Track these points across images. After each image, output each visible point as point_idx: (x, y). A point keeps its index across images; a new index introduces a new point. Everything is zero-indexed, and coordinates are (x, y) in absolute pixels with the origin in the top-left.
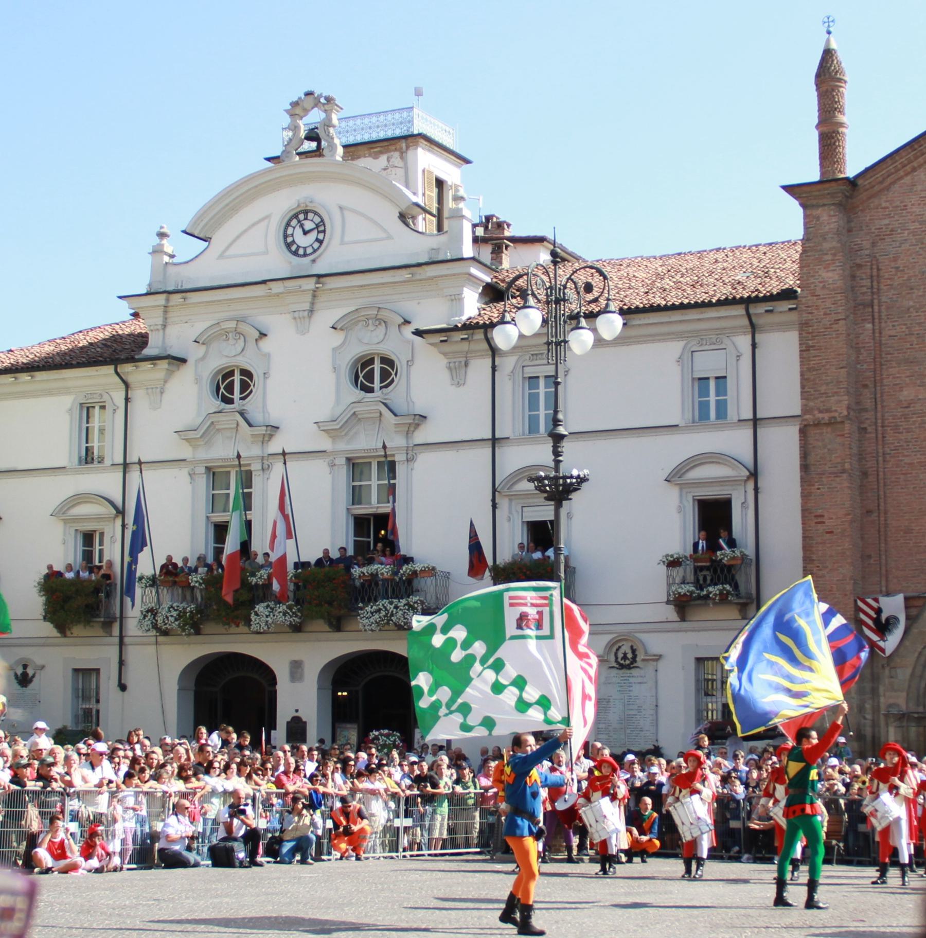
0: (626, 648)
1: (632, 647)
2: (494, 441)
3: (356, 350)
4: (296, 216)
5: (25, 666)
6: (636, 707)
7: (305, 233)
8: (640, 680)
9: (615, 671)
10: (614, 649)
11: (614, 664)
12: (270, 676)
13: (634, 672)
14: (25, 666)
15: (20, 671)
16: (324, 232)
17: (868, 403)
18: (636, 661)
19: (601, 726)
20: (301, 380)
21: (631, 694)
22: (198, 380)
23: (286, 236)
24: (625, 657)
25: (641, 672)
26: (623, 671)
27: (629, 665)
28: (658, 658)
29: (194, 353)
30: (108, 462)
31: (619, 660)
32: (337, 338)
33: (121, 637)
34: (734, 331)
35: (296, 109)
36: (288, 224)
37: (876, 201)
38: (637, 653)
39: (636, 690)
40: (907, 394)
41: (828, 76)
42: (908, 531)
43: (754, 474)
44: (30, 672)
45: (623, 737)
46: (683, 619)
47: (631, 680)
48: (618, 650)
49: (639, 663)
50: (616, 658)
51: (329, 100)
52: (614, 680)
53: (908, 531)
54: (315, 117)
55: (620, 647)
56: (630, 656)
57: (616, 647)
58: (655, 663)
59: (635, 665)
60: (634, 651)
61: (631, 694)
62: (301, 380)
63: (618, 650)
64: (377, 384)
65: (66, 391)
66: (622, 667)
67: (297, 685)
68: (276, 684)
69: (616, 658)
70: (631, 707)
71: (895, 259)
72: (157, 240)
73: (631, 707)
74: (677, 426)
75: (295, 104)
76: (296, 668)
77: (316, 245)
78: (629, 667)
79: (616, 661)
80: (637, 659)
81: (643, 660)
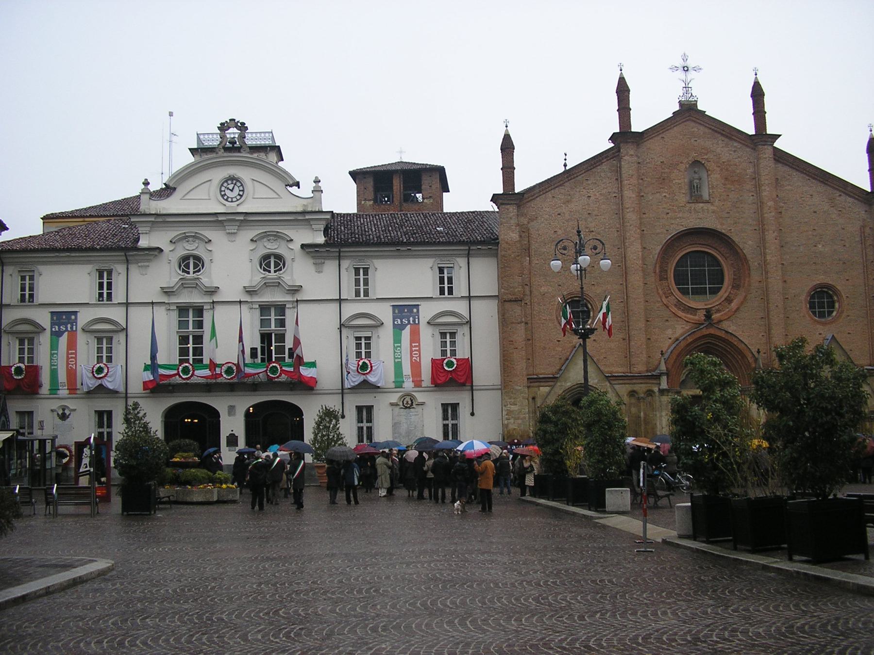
0: (408, 399)
2: (340, 301)
3: (263, 251)
4: (226, 181)
5: (64, 410)
7: (232, 191)
12: (216, 414)
14: (64, 410)
15: (60, 412)
16: (243, 191)
17: (528, 293)
20: (231, 266)
22: (170, 262)
23: (221, 191)
24: (407, 403)
28: (422, 404)
29: (166, 247)
30: (115, 301)
32: (253, 246)
33: (126, 393)
34: (459, 256)
35: (223, 127)
36: (222, 185)
37: (529, 204)
40: (543, 289)
41: (507, 147)
42: (545, 348)
43: (469, 322)
44: (67, 412)
49: (414, 406)
51: (243, 124)
53: (545, 348)
54: (233, 133)
62: (231, 266)
64: (272, 269)
65: (89, 262)
66: (406, 408)
67: (231, 418)
68: (219, 416)
71: (538, 230)
72: (143, 187)
75: (222, 124)
76: (232, 410)
77: (238, 197)
78: (409, 408)
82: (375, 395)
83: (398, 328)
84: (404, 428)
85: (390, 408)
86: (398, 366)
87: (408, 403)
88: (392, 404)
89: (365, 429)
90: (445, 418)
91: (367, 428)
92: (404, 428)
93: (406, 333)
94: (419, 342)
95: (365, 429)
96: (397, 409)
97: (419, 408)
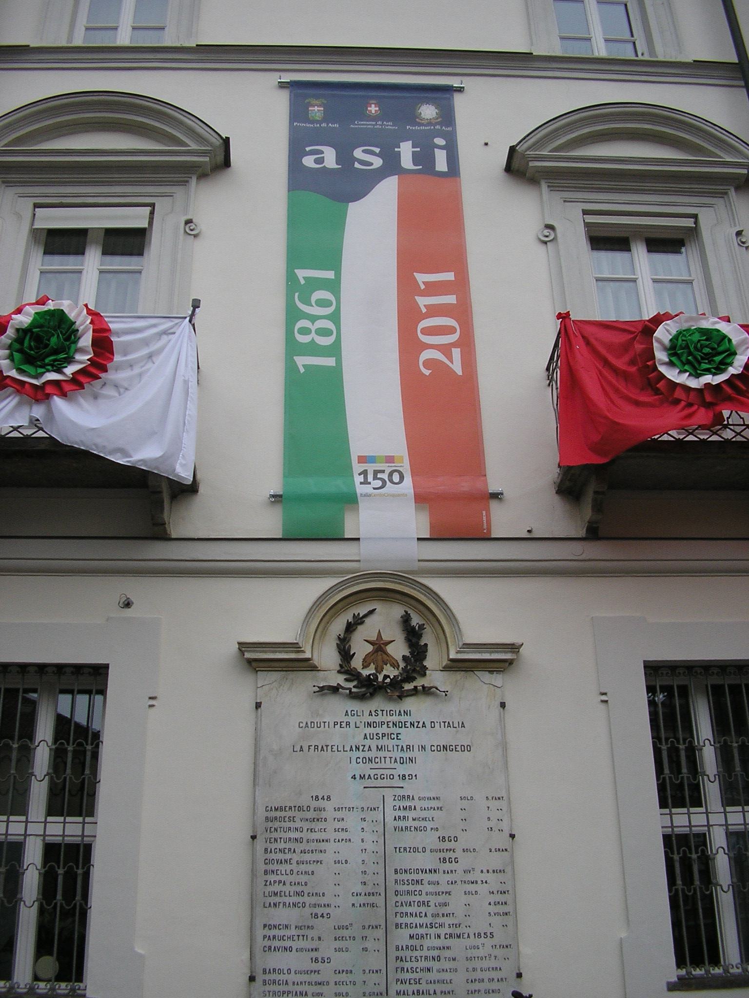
1: (406, 620)
8: (444, 736)
10: (338, 626)
11: (339, 679)
19: (281, 915)
25: (450, 710)
26: (377, 703)
31: (357, 663)
38: (428, 638)
39: (429, 775)
45: (376, 961)
46: (593, 534)
47: (408, 736)
48: (350, 628)
49: (435, 678)
50: (346, 655)
55: (359, 621)
56: (399, 650)
57: (347, 617)
58: (497, 679)
59: (419, 682)
60: (413, 635)
61: (409, 789)
63: (350, 628)
66: (368, 688)
69: (346, 655)
70: (409, 839)
73: (409, 839)
74: (526, 57)
78: (395, 689)
79: (346, 669)
80: (432, 661)
81: (456, 666)
82: (131, 587)
83: (321, 193)
84: (345, 860)
85: (243, 690)
86: (313, 400)
87: (388, 655)
89: (33, 855)
90: (677, 786)
91: (51, 851)
92: (345, 860)
93: (373, 223)
94: (456, 260)
95: (33, 855)
96: (292, 700)
97: (474, 697)
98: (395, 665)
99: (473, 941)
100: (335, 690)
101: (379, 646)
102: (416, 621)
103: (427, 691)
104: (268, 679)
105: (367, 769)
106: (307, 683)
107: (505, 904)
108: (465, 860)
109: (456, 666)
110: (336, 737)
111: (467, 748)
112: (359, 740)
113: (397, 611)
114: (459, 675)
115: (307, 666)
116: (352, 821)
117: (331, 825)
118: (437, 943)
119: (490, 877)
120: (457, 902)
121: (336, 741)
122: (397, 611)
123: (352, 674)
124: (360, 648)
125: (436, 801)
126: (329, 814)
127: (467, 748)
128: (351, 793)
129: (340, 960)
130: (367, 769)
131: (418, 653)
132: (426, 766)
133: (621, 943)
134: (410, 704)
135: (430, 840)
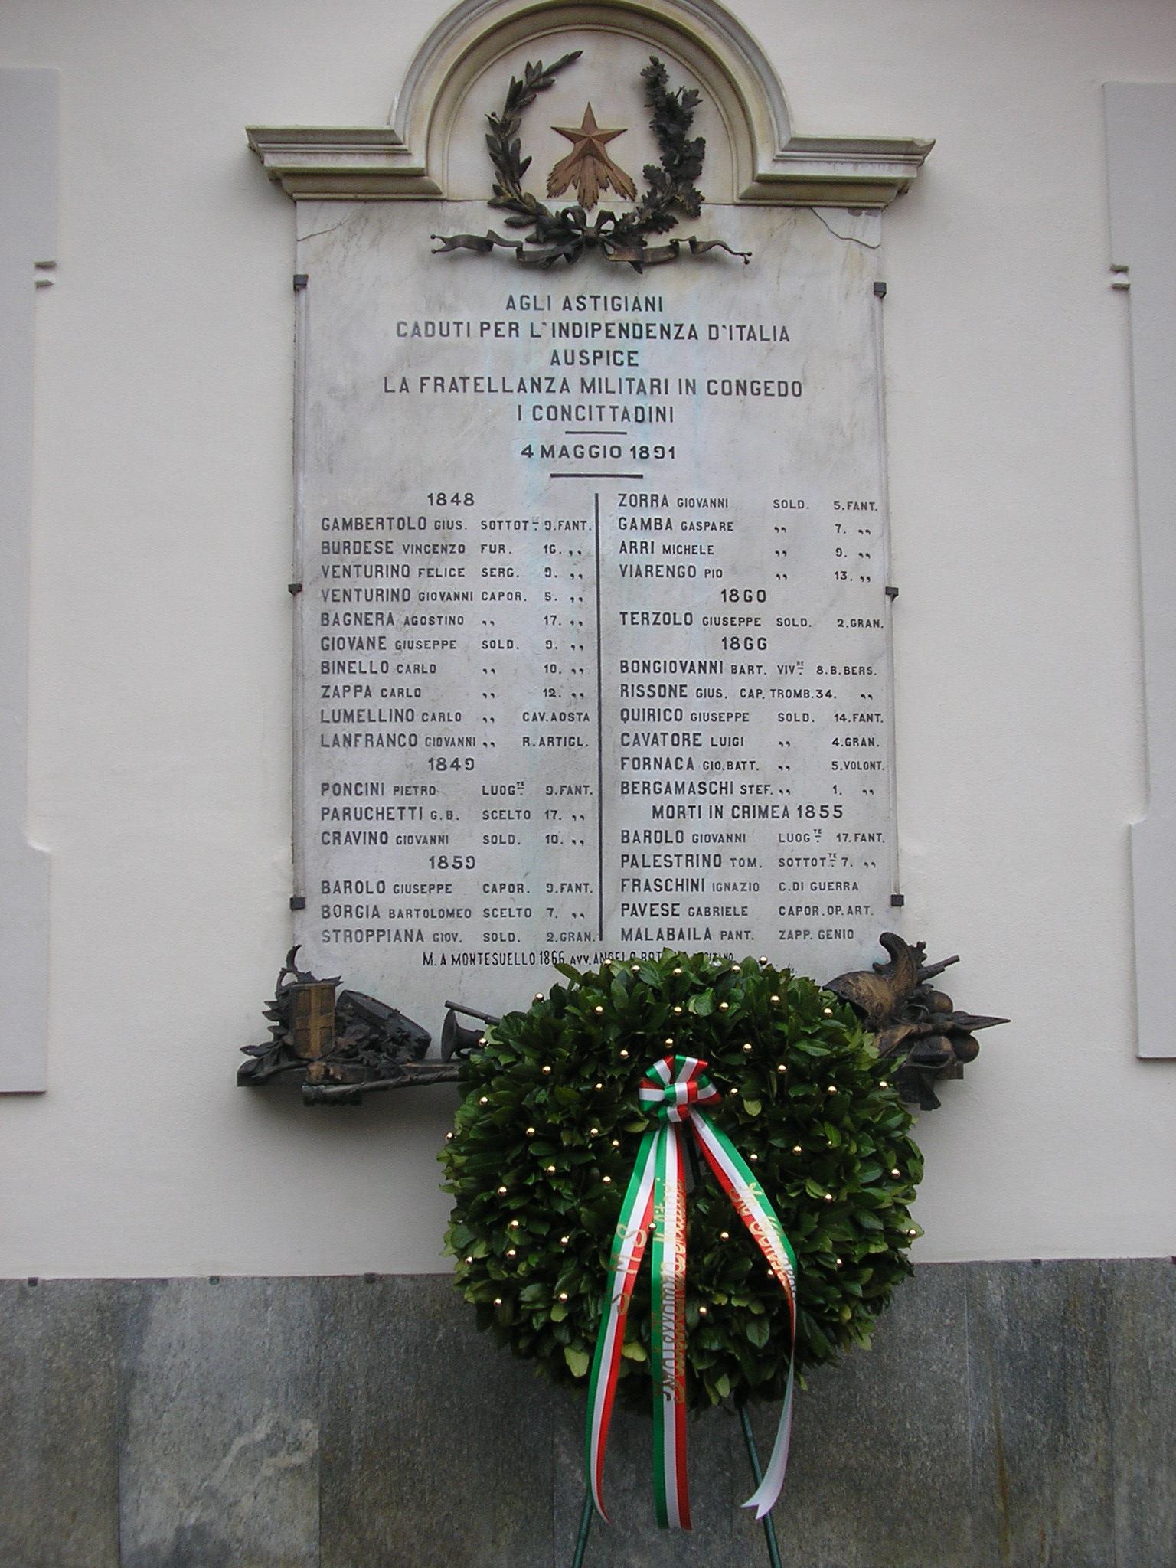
1: (654, 79)
6: (704, 596)
8: (738, 360)
9: (489, 289)
10: (489, 94)
11: (495, 222)
13: (675, 290)
18: (692, 208)
19: (359, 764)
21: (656, 478)
25: (757, 299)
26: (584, 280)
27: (627, 235)
31: (534, 184)
38: (705, 126)
45: (577, 864)
47: (656, 358)
48: (519, 98)
49: (720, 220)
50: (508, 164)
52: (485, 358)
56: (635, 153)
57: (514, 70)
58: (869, 228)
59: (684, 231)
60: (669, 118)
61: (656, 478)
63: (519, 98)
66: (561, 245)
69: (508, 164)
70: (654, 595)
73: (654, 595)
78: (628, 247)
79: (508, 196)
84: (506, 643)
85: (262, 247)
88: (299, 173)
96: (380, 272)
97: (809, 271)
98: (626, 190)
99: (796, 824)
100: (483, 246)
101: (589, 144)
102: (677, 82)
103: (700, 253)
104: (321, 221)
105: (557, 433)
106: (414, 230)
107: (869, 744)
108: (782, 646)
109: (775, 194)
110: (485, 358)
111: (792, 389)
112: (539, 365)
113: (632, 59)
114: (778, 218)
115: (414, 189)
116: (524, 553)
117: (475, 561)
118: (717, 826)
119: (837, 683)
120: (761, 738)
121: (485, 367)
122: (632, 59)
123: (523, 212)
124: (543, 148)
125: (718, 509)
126: (471, 535)
127: (792, 389)
128: (522, 488)
129: (495, 862)
130: (557, 433)
131: (681, 160)
132: (698, 430)
133: (1129, 839)
134: (661, 282)
135: (704, 596)
